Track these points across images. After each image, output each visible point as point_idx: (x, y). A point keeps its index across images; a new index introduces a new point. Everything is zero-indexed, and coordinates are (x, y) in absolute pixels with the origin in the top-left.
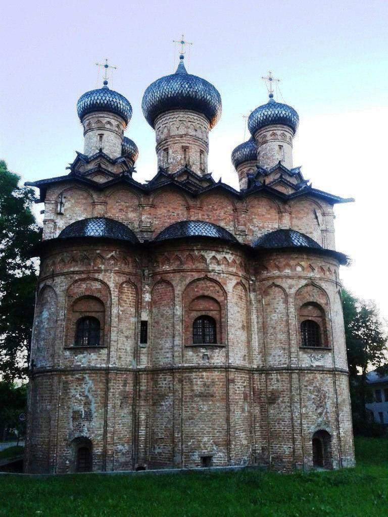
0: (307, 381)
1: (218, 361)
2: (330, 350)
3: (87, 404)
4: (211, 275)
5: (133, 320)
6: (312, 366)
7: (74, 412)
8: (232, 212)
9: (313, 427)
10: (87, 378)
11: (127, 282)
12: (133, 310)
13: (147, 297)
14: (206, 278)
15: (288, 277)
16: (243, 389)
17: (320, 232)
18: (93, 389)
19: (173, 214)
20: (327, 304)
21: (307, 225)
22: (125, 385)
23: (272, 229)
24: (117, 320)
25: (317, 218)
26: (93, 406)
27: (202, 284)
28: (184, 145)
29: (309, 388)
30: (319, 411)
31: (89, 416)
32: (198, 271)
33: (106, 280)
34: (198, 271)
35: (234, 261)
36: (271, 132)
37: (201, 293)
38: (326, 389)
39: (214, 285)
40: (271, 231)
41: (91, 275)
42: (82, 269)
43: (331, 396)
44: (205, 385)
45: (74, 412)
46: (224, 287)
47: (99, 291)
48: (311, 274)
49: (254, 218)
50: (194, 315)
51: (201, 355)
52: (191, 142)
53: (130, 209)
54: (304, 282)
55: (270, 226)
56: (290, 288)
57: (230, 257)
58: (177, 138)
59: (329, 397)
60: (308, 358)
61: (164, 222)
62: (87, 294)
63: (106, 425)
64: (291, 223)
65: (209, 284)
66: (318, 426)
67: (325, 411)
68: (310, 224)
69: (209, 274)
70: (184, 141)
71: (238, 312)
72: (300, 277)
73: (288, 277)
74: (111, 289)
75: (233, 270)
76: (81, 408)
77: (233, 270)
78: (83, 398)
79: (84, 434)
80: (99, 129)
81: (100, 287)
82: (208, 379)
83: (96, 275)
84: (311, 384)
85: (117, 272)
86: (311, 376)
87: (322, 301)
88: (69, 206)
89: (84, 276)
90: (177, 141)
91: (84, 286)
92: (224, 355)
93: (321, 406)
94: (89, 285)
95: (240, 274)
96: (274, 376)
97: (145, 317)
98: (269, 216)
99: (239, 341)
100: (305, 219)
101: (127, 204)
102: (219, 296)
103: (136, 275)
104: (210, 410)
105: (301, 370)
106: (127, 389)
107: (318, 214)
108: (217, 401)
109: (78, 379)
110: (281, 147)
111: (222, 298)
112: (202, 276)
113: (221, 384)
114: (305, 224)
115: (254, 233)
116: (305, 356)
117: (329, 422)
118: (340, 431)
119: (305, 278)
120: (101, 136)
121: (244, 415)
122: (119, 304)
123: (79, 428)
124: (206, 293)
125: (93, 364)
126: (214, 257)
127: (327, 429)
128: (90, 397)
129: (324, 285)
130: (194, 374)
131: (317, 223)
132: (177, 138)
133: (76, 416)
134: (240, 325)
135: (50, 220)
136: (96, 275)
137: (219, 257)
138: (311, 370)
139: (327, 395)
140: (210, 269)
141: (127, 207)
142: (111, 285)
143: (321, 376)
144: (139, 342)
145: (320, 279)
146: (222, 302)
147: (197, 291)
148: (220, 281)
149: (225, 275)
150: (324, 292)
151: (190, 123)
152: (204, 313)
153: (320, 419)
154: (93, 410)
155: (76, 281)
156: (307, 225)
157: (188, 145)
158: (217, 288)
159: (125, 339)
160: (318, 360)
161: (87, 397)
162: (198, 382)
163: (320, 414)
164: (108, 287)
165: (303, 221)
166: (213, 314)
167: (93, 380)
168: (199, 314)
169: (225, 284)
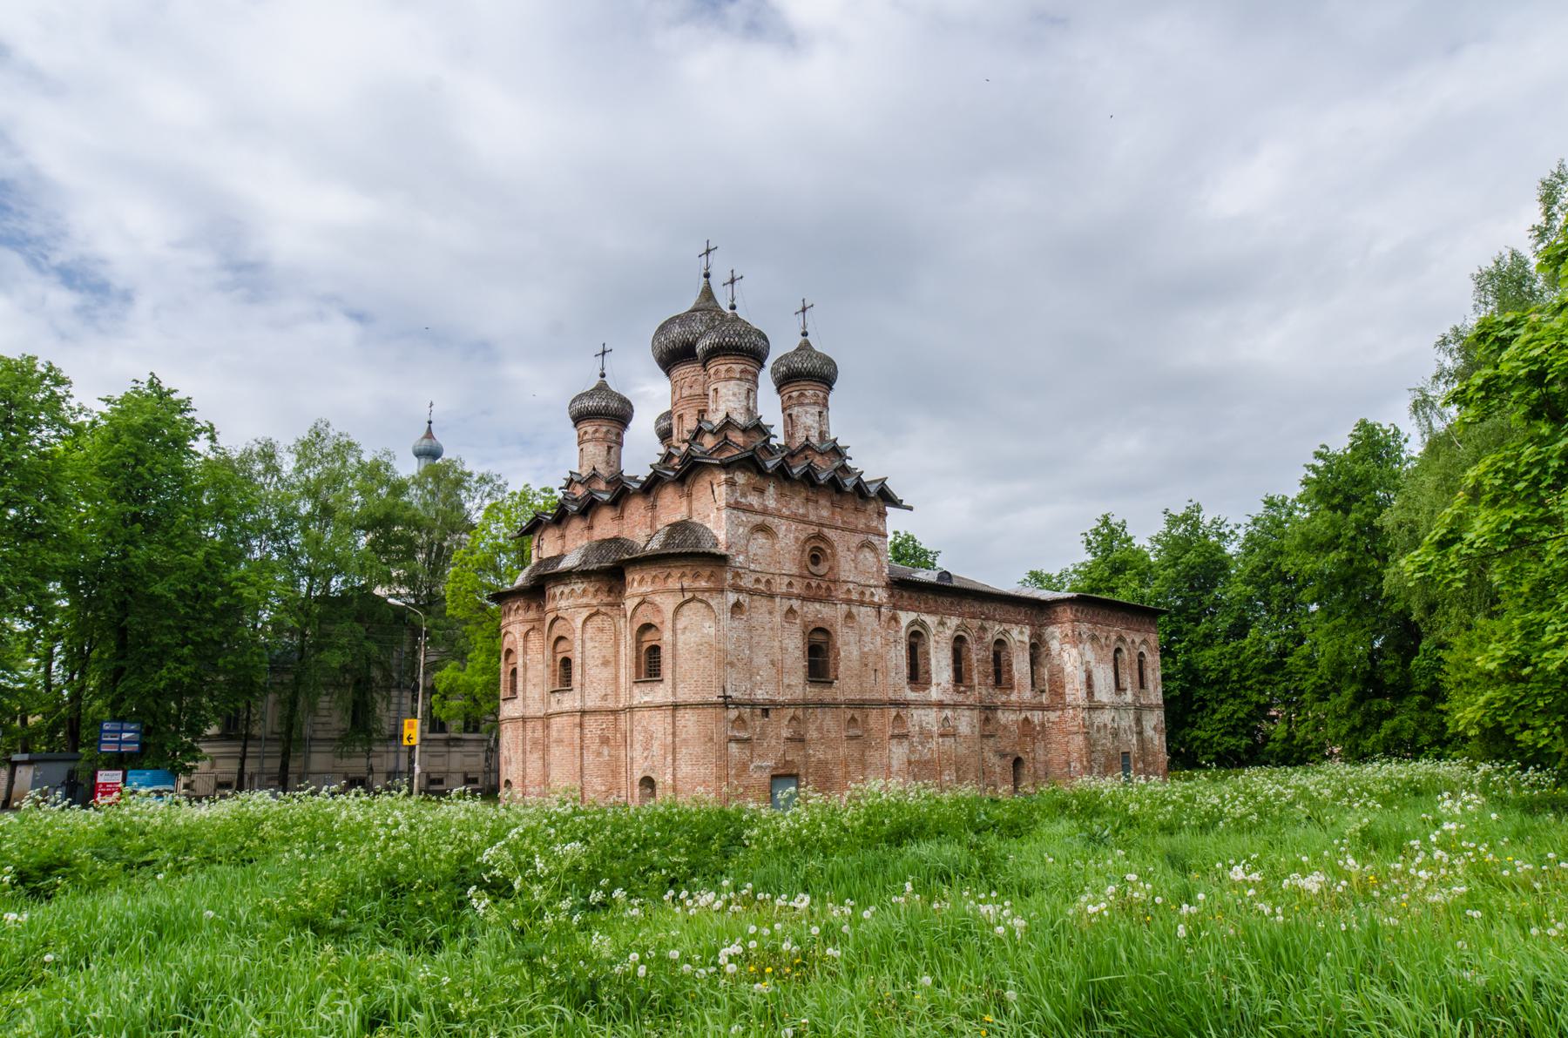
2: (661, 681)
4: (561, 614)
11: (533, 629)
14: (557, 618)
20: (662, 623)
27: (558, 624)
35: (584, 591)
38: (654, 728)
48: (644, 589)
50: (559, 657)
54: (637, 600)
57: (579, 587)
64: (690, 510)
75: (584, 600)
77: (584, 600)
87: (655, 621)
95: (594, 602)
103: (539, 620)
105: (631, 709)
110: (716, 390)
122: (525, 652)
126: (562, 593)
129: (658, 599)
134: (599, 662)
137: (567, 590)
142: (517, 636)
145: (653, 592)
150: (658, 610)
160: (646, 694)
162: (556, 723)
166: (568, 655)
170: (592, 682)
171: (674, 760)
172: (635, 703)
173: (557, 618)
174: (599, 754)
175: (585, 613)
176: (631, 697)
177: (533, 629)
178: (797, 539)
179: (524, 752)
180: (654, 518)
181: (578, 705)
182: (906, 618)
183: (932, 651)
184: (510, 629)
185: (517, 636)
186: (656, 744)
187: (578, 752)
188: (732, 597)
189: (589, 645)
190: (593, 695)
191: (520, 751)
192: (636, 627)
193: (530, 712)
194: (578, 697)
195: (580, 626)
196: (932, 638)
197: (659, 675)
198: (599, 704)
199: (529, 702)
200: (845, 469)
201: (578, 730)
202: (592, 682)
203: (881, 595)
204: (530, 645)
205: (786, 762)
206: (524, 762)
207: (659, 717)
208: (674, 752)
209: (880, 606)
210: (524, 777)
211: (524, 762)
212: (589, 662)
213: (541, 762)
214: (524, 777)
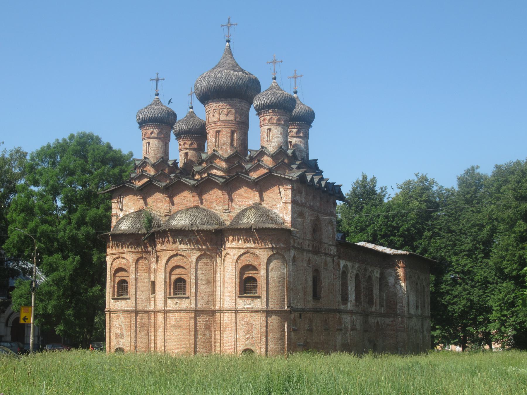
0: (241, 318)
1: (184, 306)
3: (121, 330)
4: (179, 252)
5: (147, 280)
6: (244, 308)
7: (116, 334)
8: (221, 195)
9: (242, 346)
10: (121, 315)
12: (146, 275)
13: (153, 266)
14: (177, 255)
15: (233, 248)
16: (204, 322)
17: (282, 203)
18: (124, 321)
19: (184, 201)
20: (260, 265)
21: (273, 199)
22: (142, 320)
23: (248, 205)
24: (134, 281)
25: (280, 193)
26: (124, 331)
27: (176, 258)
28: (217, 130)
29: (242, 322)
30: (247, 337)
31: (123, 336)
32: (172, 250)
33: (128, 258)
34: (172, 250)
36: (263, 117)
37: (174, 265)
39: (183, 258)
40: (247, 206)
41: (120, 256)
42: (116, 252)
43: (257, 326)
44: (176, 320)
45: (116, 334)
46: (189, 259)
47: (125, 264)
49: (236, 198)
50: (174, 278)
51: (175, 302)
52: (222, 126)
53: (159, 201)
54: (242, 251)
55: (246, 203)
56: (234, 256)
58: (212, 125)
59: (255, 328)
60: (243, 303)
61: (179, 208)
62: (120, 266)
63: (131, 342)
65: (179, 257)
66: (245, 346)
67: (251, 337)
68: (275, 198)
69: (179, 251)
70: (217, 127)
71: (203, 274)
72: (240, 248)
73: (233, 248)
74: (131, 263)
76: (118, 332)
78: (120, 327)
79: (121, 346)
80: (147, 138)
81: (125, 262)
82: (178, 317)
83: (123, 255)
84: (243, 319)
85: (133, 252)
86: (243, 314)
87: (255, 263)
88: (125, 202)
89: (117, 256)
90: (212, 128)
91: (118, 262)
92: (189, 302)
93: (248, 334)
94: (120, 261)
96: (226, 314)
97: (152, 279)
98: (246, 195)
99: (202, 292)
100: (271, 194)
101: (157, 197)
102: (186, 265)
104: (178, 335)
106: (143, 321)
107: (281, 189)
108: (183, 330)
109: (118, 316)
110: (270, 130)
111: (188, 267)
112: (175, 253)
113: (186, 320)
114: (271, 199)
115: (236, 210)
116: (241, 301)
117: (254, 343)
118: (262, 350)
119: (243, 248)
120: (149, 143)
121: (205, 338)
123: (118, 342)
124: (178, 264)
125: (123, 308)
127: (253, 348)
128: (123, 326)
129: (258, 252)
130: (171, 314)
131: (280, 197)
132: (212, 125)
133: (117, 336)
135: (115, 214)
136: (123, 255)
138: (242, 311)
139: (254, 326)
140: (179, 248)
141: (157, 199)
142: (131, 261)
143: (251, 314)
144: (150, 294)
145: (255, 248)
146: (188, 268)
147: (174, 263)
148: (186, 255)
149: (190, 251)
151: (221, 110)
152: (179, 276)
153: (247, 342)
154: (124, 333)
155: (114, 259)
156: (273, 199)
157: (220, 129)
158: (185, 260)
159: (141, 293)
161: (121, 326)
163: (248, 339)
164: (130, 262)
165: (270, 196)
166: (183, 277)
167: (124, 316)
168: (176, 277)
169: (190, 257)
170: (201, 294)
171: (267, 340)
172: (239, 308)
173: (177, 255)
174: (204, 335)
175: (198, 254)
176: (236, 304)
177: (141, 258)
178: (311, 220)
179: (136, 331)
180: (231, 200)
181: (193, 306)
182: (342, 263)
183: (349, 282)
184: (124, 256)
185: (131, 261)
186: (255, 332)
187: (193, 333)
188: (293, 253)
189: (199, 272)
190: (202, 301)
191: (133, 331)
192: (240, 266)
193: (140, 307)
194: (193, 302)
195: (194, 261)
196: (349, 275)
197: (256, 292)
198: (205, 306)
199: (139, 301)
200: (322, 179)
201: (193, 321)
202: (201, 294)
203: (334, 250)
204: (140, 267)
205: (307, 343)
206: (136, 337)
207: (257, 317)
208: (267, 337)
209: (334, 256)
210: (136, 347)
211: (136, 337)
212: (199, 282)
213: (147, 338)
214: (136, 347)
